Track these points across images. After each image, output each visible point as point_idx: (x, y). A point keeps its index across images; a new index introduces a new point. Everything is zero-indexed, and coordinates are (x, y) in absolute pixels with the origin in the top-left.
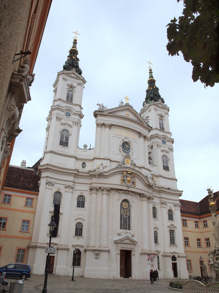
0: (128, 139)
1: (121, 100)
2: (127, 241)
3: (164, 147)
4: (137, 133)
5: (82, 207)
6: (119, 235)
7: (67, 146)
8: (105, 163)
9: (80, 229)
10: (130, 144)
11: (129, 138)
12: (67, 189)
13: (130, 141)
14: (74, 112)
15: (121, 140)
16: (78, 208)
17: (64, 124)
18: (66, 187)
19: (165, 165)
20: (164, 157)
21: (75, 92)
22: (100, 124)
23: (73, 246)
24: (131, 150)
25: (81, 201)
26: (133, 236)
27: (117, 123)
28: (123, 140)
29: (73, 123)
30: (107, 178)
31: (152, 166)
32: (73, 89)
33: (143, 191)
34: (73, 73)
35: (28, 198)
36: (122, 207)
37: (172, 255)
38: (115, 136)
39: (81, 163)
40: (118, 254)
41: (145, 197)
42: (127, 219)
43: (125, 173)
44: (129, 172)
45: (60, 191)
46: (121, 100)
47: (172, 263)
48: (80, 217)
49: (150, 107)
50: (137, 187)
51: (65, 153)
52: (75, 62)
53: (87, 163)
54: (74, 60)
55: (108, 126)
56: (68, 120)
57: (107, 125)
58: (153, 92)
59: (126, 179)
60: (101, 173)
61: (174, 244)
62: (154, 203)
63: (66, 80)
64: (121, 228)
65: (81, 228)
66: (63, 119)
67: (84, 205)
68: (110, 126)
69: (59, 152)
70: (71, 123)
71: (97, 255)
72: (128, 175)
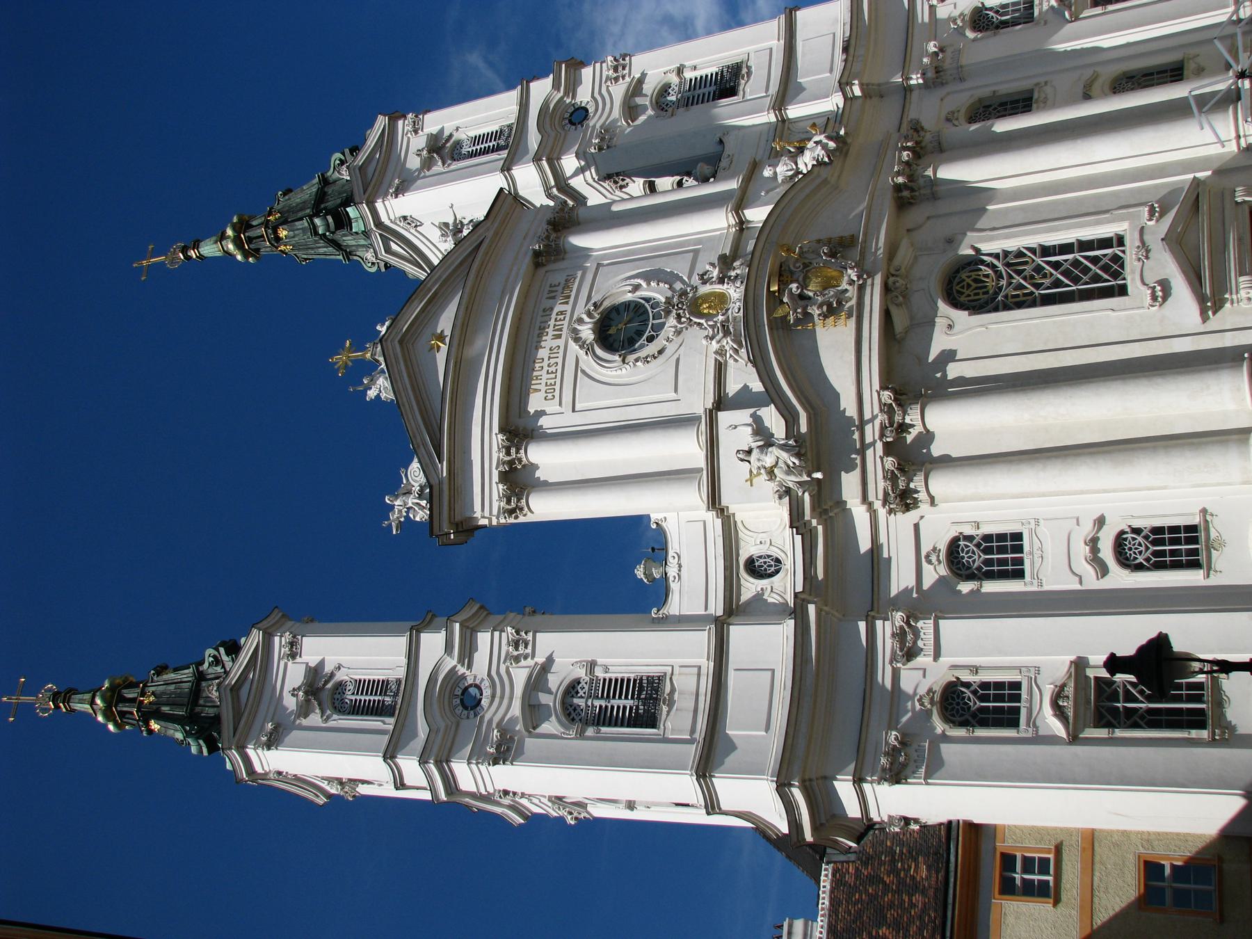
4: (542, 271)
5: (1020, 549)
7: (661, 679)
9: (1154, 543)
10: (607, 304)
15: (587, 362)
28: (589, 350)
31: (724, 163)
44: (775, 288)
48: (1082, 551)
49: (387, 222)
53: (749, 548)
54: (163, 693)
58: (305, 223)
60: (798, 455)
64: (1122, 291)
65: (1146, 537)
67: (1001, 537)
70: (520, 676)
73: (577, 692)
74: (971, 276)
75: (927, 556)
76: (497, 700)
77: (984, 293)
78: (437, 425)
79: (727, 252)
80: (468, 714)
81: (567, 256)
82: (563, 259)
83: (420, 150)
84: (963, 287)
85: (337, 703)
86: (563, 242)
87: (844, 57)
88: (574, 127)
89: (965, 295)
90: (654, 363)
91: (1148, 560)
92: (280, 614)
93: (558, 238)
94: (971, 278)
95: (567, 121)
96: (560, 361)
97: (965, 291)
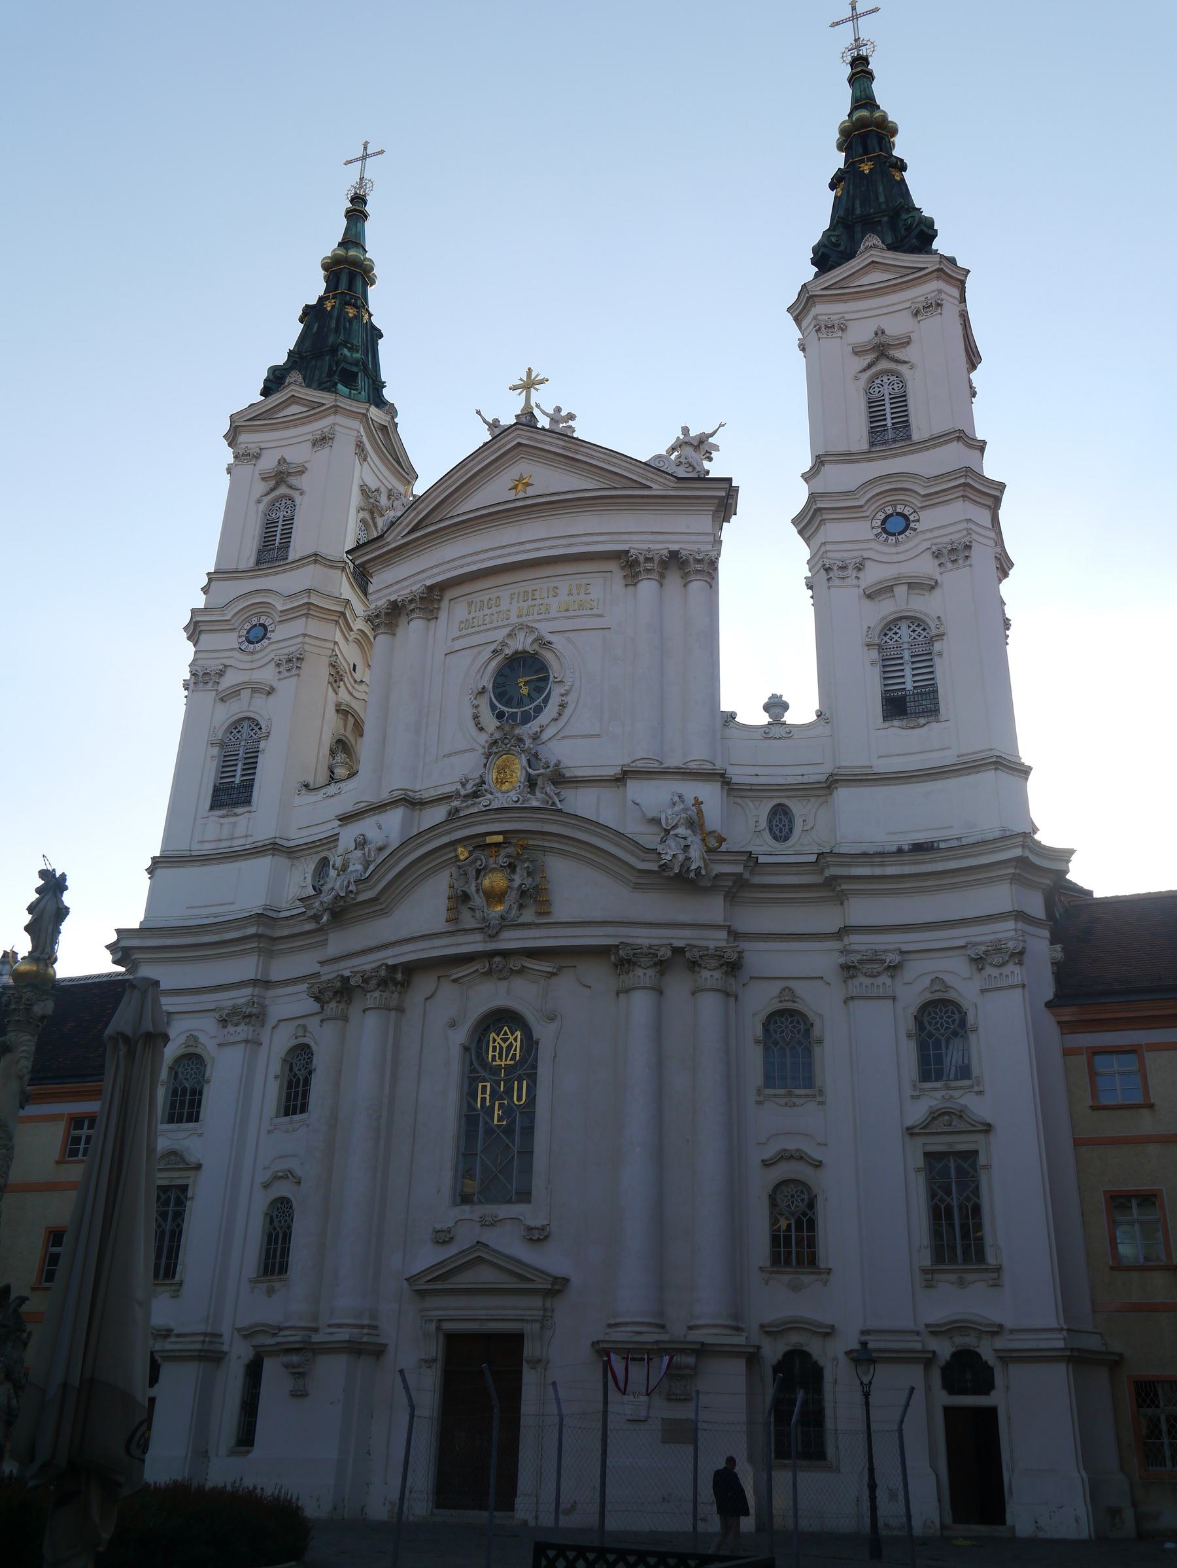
0: (532, 630)
1: (478, 412)
2: (485, 1276)
3: (901, 557)
6: (444, 1242)
8: (368, 827)
11: (534, 625)
12: (231, 1029)
13: (549, 637)
14: (280, 608)
15: (487, 653)
16: (287, 1119)
17: (235, 692)
18: (224, 1022)
19: (909, 686)
20: (905, 631)
21: (302, 494)
22: (377, 616)
23: (248, 1334)
24: (557, 692)
25: (301, 1076)
26: (538, 1237)
27: (448, 570)
29: (281, 669)
30: (384, 912)
32: (291, 487)
33: (611, 930)
34: (293, 400)
35: (77, 1121)
36: (485, 1065)
37: (945, 1349)
38: (458, 645)
39: (308, 867)
40: (426, 1361)
41: (635, 964)
42: (509, 1131)
43: (463, 852)
44: (489, 840)
45: (198, 1050)
46: (478, 412)
47: (948, 1411)
50: (563, 910)
51: (236, 842)
52: (333, 325)
55: (413, 606)
56: (255, 665)
57: (411, 601)
59: (473, 889)
60: (337, 897)
61: (981, 1257)
62: (781, 984)
63: (257, 457)
66: (229, 672)
68: (432, 601)
69: (208, 848)
71: (299, 1374)
72: (483, 858)
73: (252, 730)
74: (516, 1041)
75: (304, 1027)
76: (249, 658)
77: (494, 1056)
78: (443, 517)
79: (566, 776)
80: (243, 636)
81: (631, 589)
82: (626, 585)
83: (883, 332)
84: (506, 1033)
85: (277, 504)
86: (642, 580)
87: (906, 848)
88: (879, 523)
89: (496, 1037)
90: (471, 724)
91: (275, 1229)
92: (365, 412)
93: (648, 571)
94: (513, 1042)
95: (889, 512)
96: (495, 624)
97: (501, 1036)
